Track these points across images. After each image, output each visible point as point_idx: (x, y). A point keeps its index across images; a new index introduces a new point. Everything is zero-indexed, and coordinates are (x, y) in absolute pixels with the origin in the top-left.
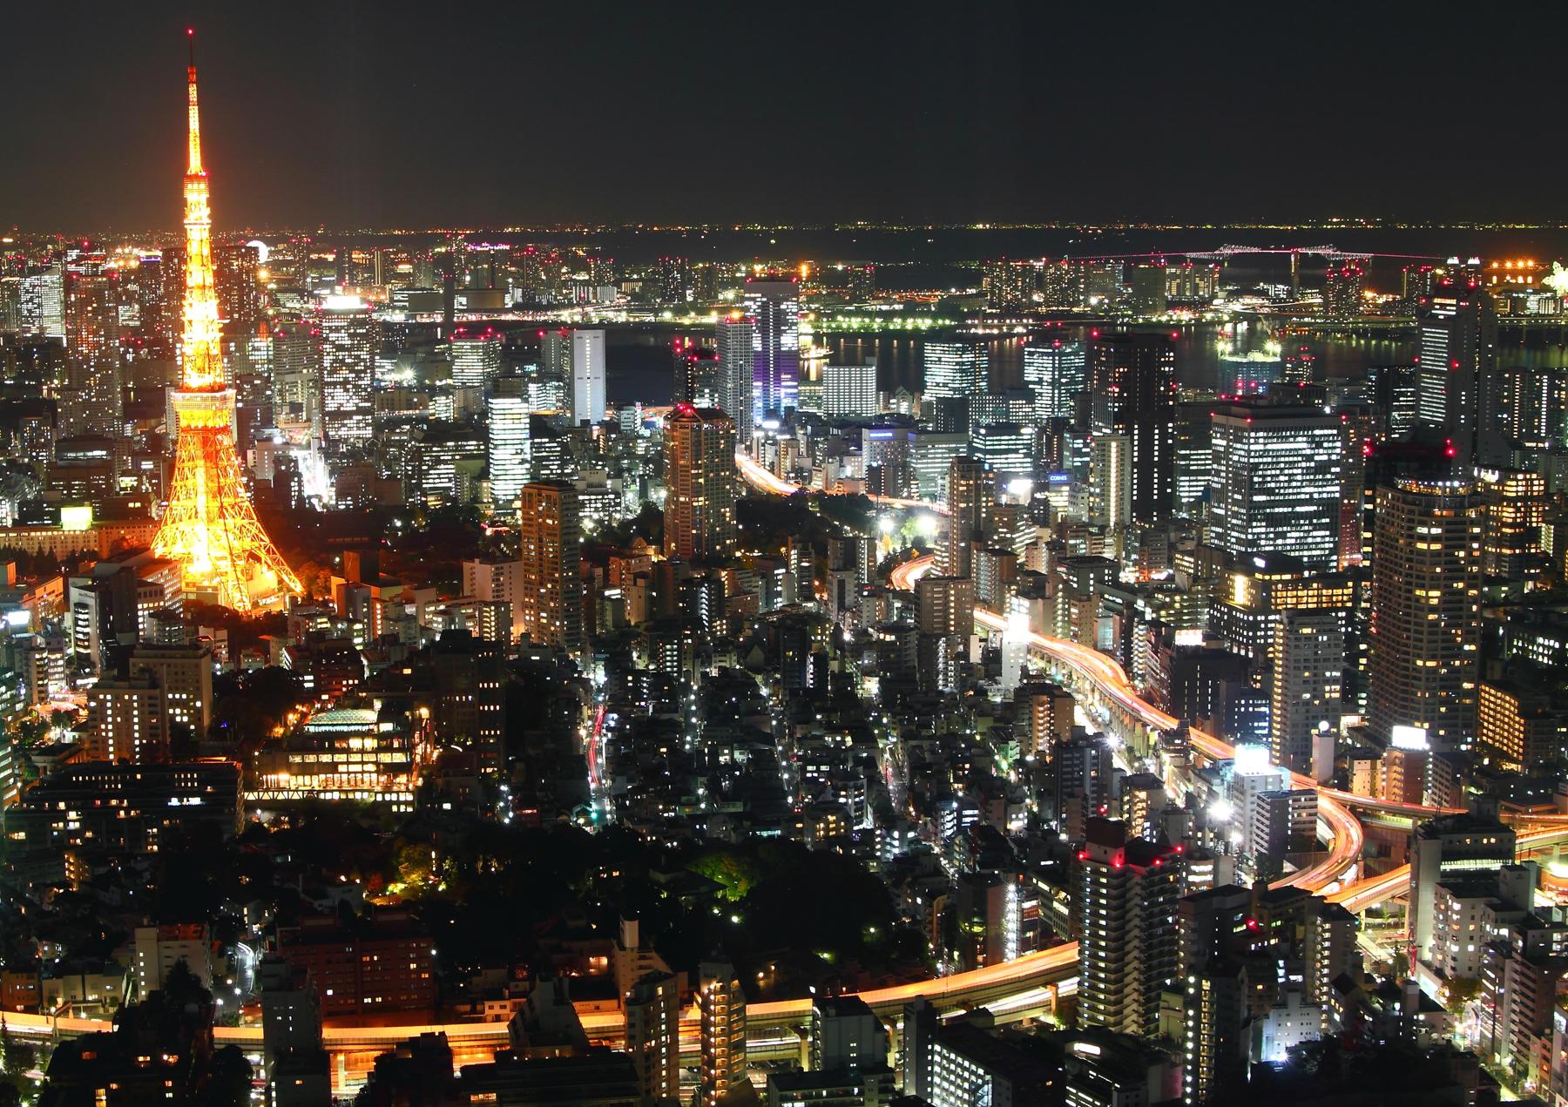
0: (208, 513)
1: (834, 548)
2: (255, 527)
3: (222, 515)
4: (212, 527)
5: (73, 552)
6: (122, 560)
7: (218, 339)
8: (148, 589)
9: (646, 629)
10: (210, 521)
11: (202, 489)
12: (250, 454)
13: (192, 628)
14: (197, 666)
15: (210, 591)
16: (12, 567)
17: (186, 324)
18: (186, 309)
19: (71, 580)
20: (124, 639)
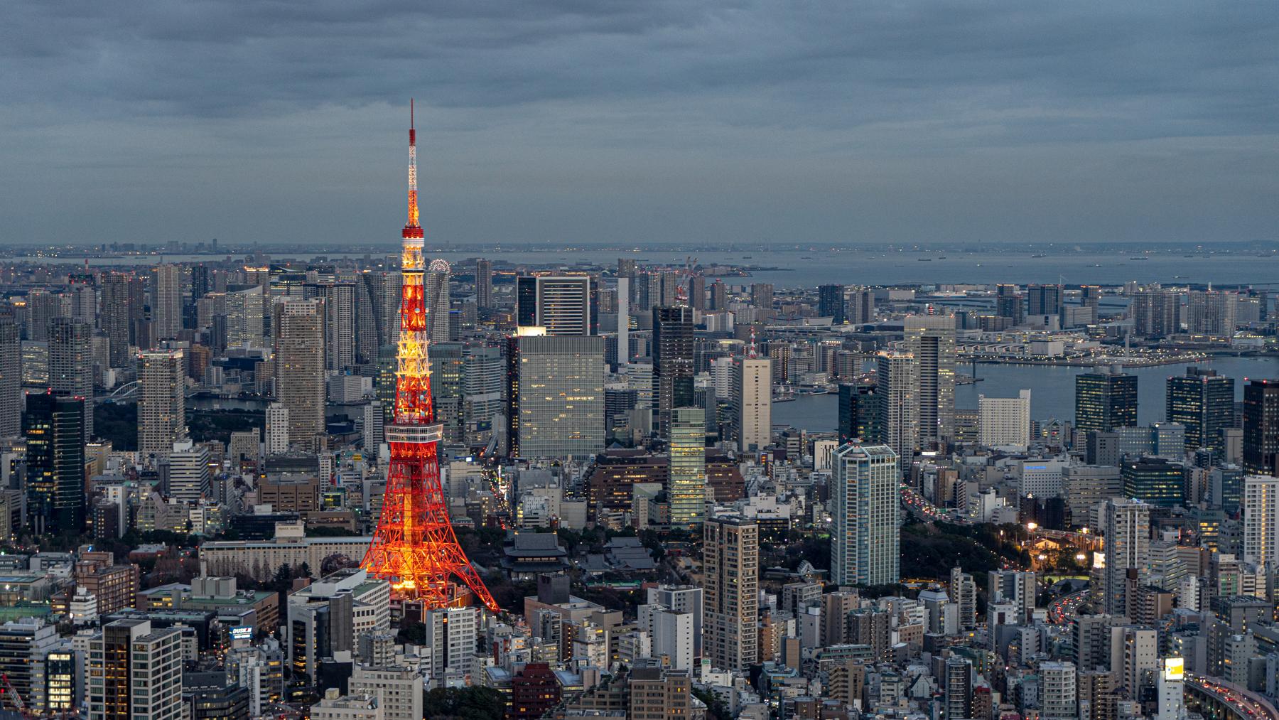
0: (414, 535)
1: (997, 578)
2: (455, 549)
3: (425, 539)
4: (417, 549)
5: (286, 565)
6: (338, 581)
7: (428, 375)
8: (361, 609)
9: (818, 657)
10: (415, 543)
11: (408, 514)
12: (443, 471)
13: (399, 648)
14: (410, 686)
15: (413, 608)
16: (233, 581)
17: (400, 362)
18: (401, 349)
19: (290, 598)
20: (342, 657)
